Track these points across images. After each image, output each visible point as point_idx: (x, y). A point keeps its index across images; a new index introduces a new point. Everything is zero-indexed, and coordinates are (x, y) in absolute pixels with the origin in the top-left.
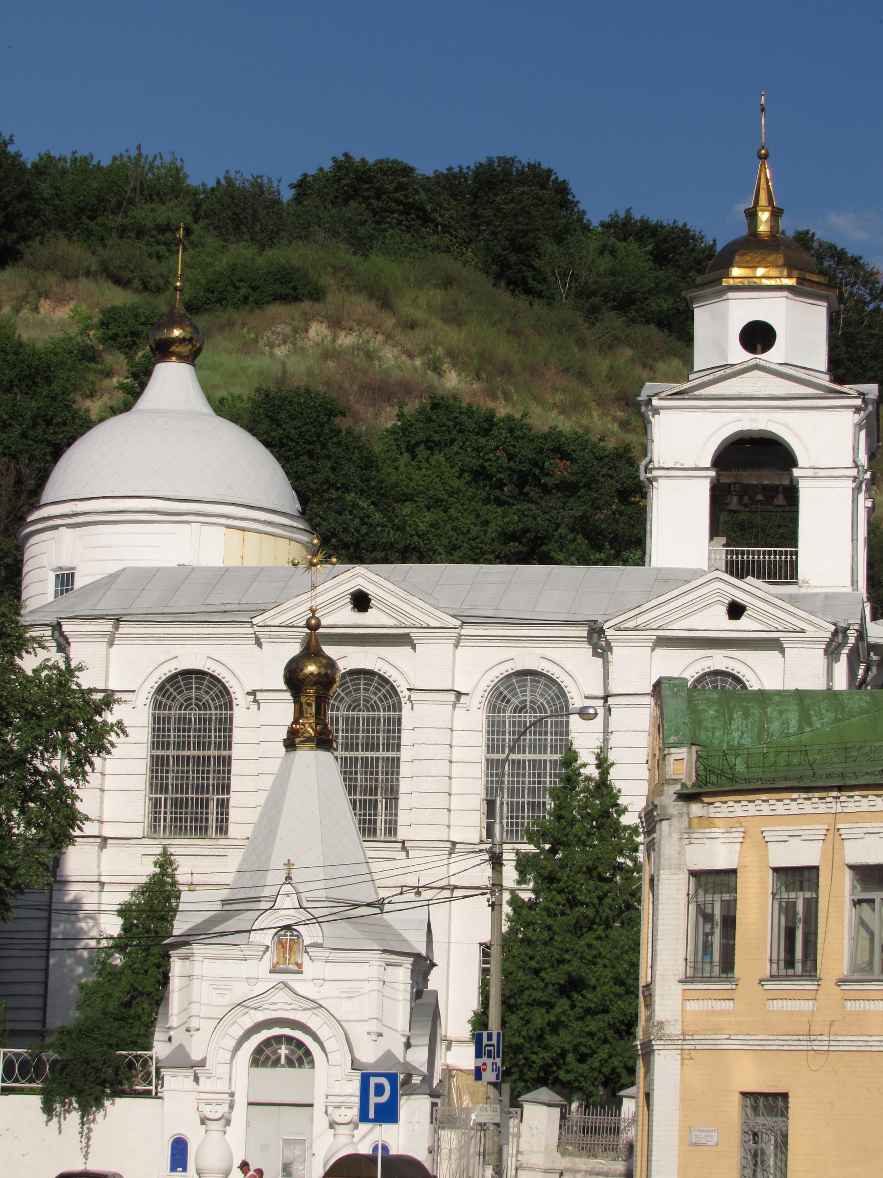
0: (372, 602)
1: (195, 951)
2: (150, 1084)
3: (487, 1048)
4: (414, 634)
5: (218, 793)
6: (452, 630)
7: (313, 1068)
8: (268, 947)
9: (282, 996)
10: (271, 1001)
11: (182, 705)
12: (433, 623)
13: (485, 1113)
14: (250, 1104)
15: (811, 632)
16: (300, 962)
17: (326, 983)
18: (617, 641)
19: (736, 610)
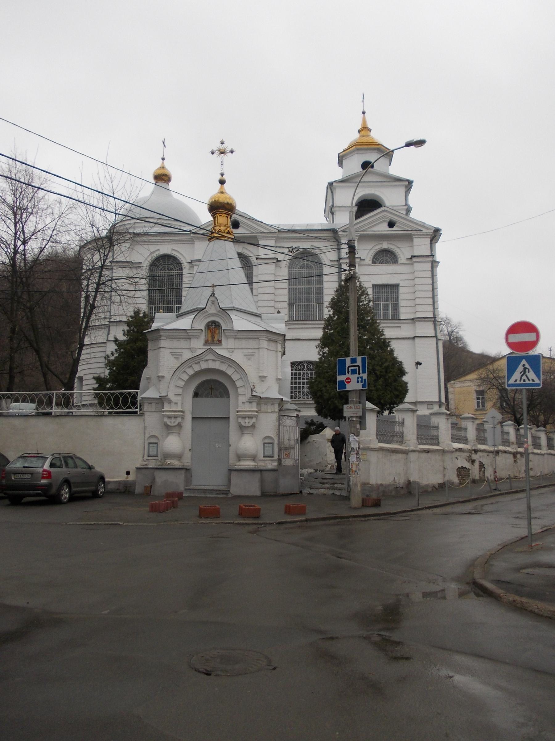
0: (240, 224)
1: (161, 334)
2: (137, 408)
3: (350, 368)
4: (259, 235)
5: (177, 304)
6: (274, 234)
7: (229, 397)
8: (202, 330)
9: (210, 357)
10: (205, 359)
11: (161, 269)
12: (266, 231)
13: (350, 410)
14: (193, 418)
15: (425, 231)
16: (220, 339)
17: (236, 351)
18: (343, 237)
19: (391, 224)
